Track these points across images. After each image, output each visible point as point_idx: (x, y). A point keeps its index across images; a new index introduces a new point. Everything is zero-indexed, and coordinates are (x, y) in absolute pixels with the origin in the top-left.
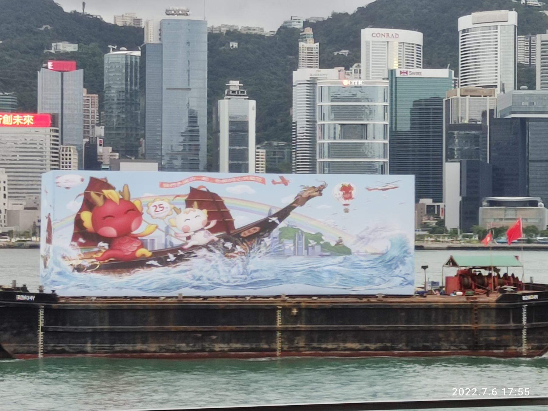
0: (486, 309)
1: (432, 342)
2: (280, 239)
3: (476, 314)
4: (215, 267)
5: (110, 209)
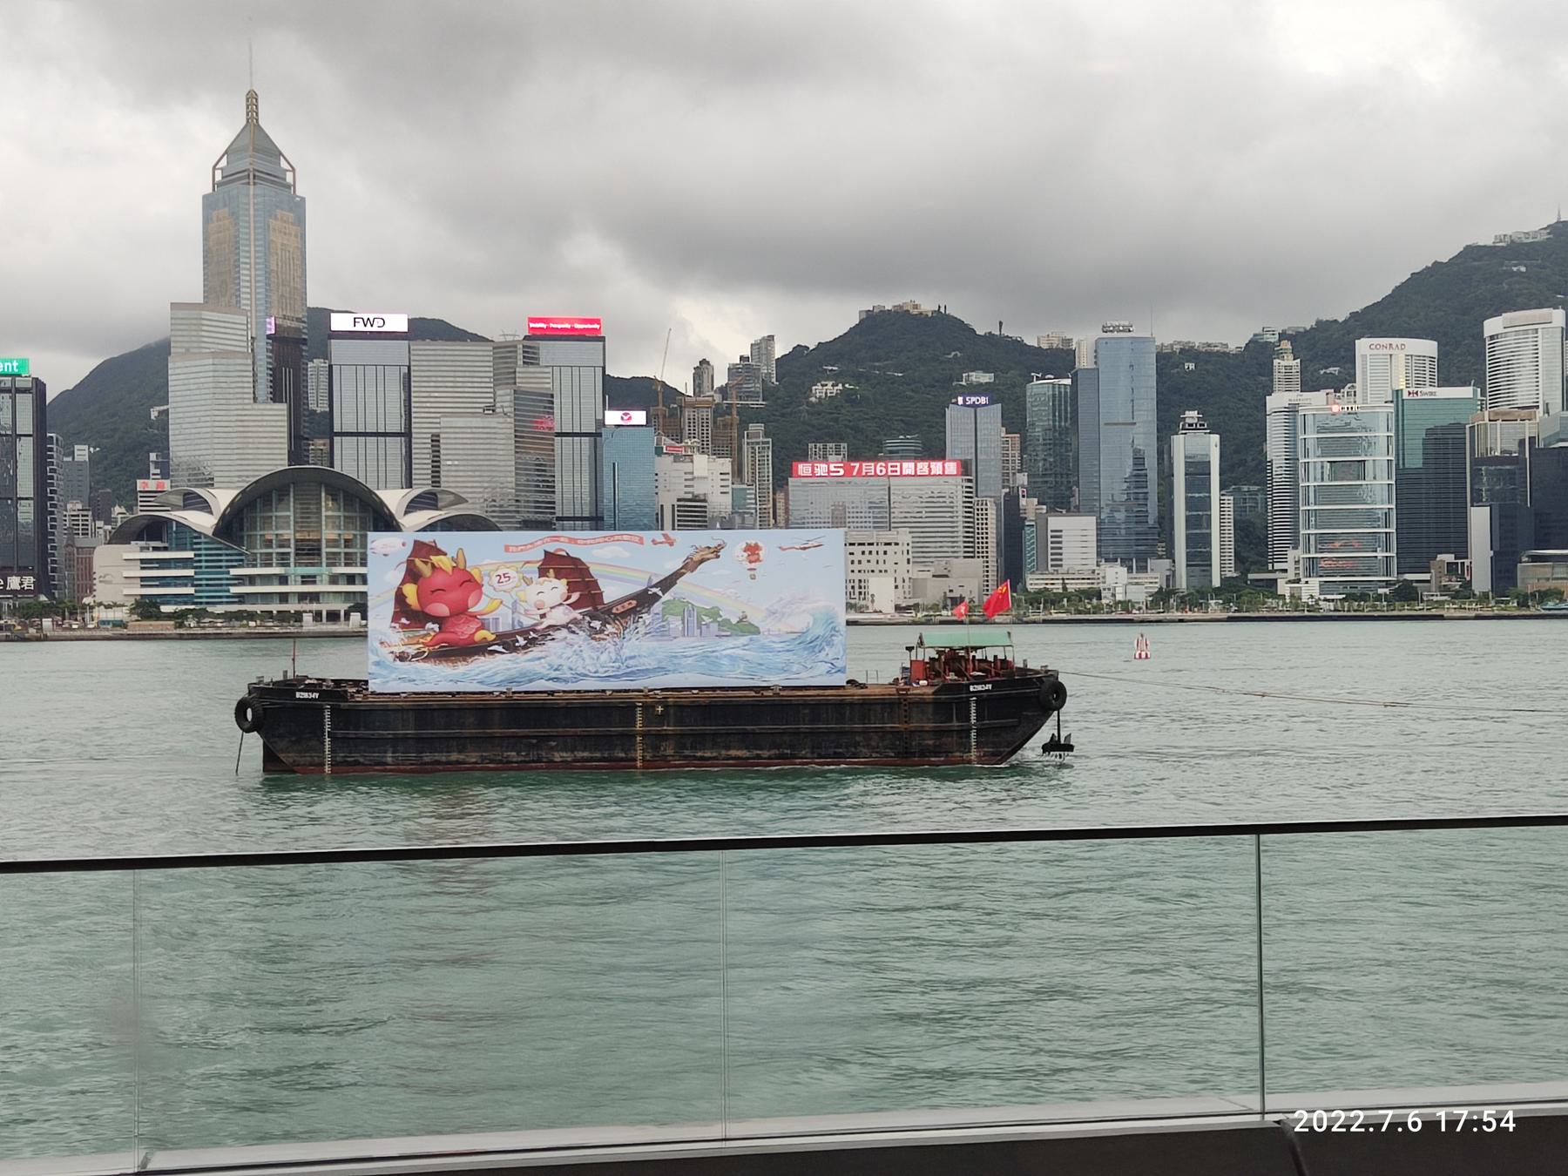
0: (920, 703)
1: (846, 747)
2: (664, 616)
3: (906, 711)
4: (579, 653)
5: (439, 580)
